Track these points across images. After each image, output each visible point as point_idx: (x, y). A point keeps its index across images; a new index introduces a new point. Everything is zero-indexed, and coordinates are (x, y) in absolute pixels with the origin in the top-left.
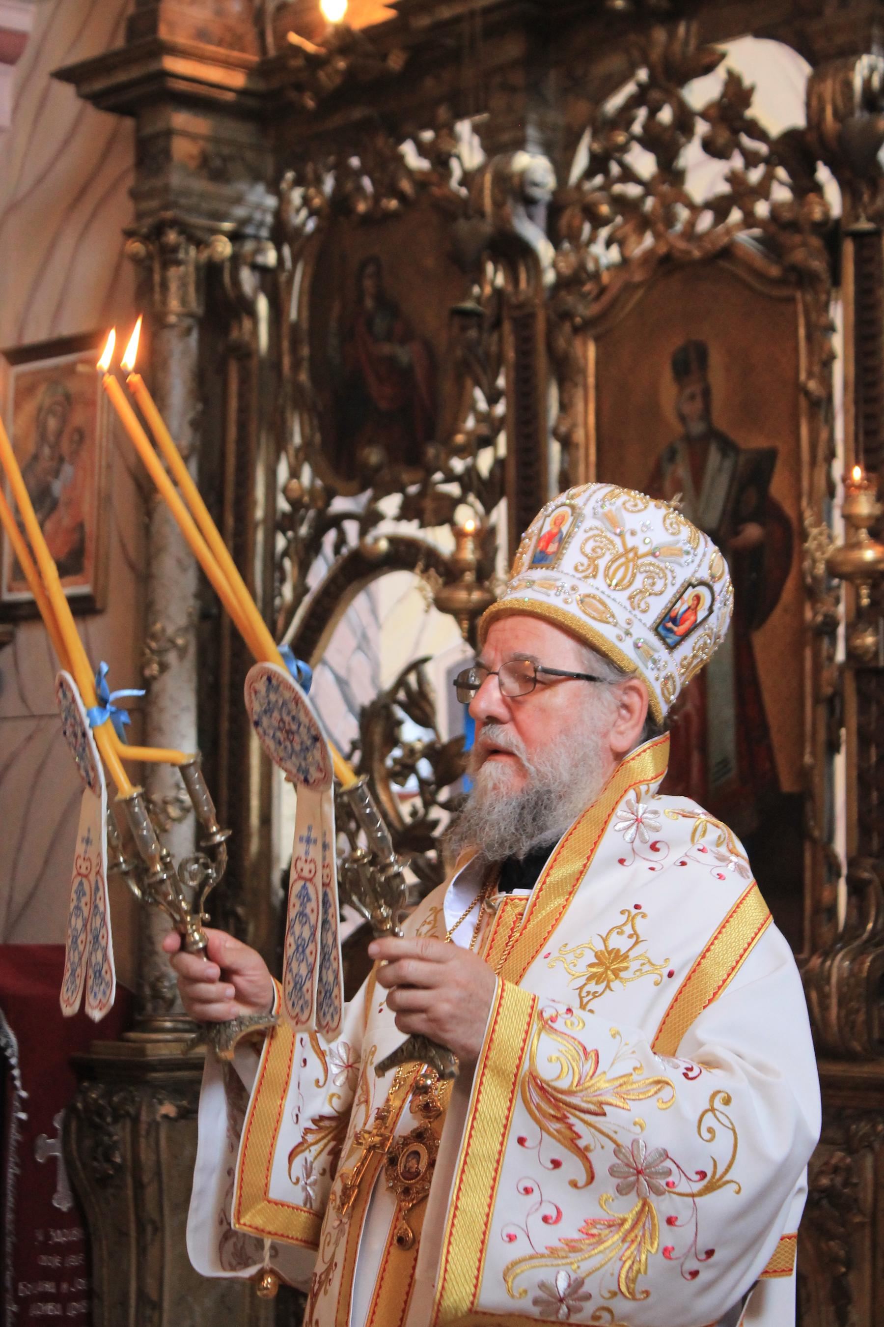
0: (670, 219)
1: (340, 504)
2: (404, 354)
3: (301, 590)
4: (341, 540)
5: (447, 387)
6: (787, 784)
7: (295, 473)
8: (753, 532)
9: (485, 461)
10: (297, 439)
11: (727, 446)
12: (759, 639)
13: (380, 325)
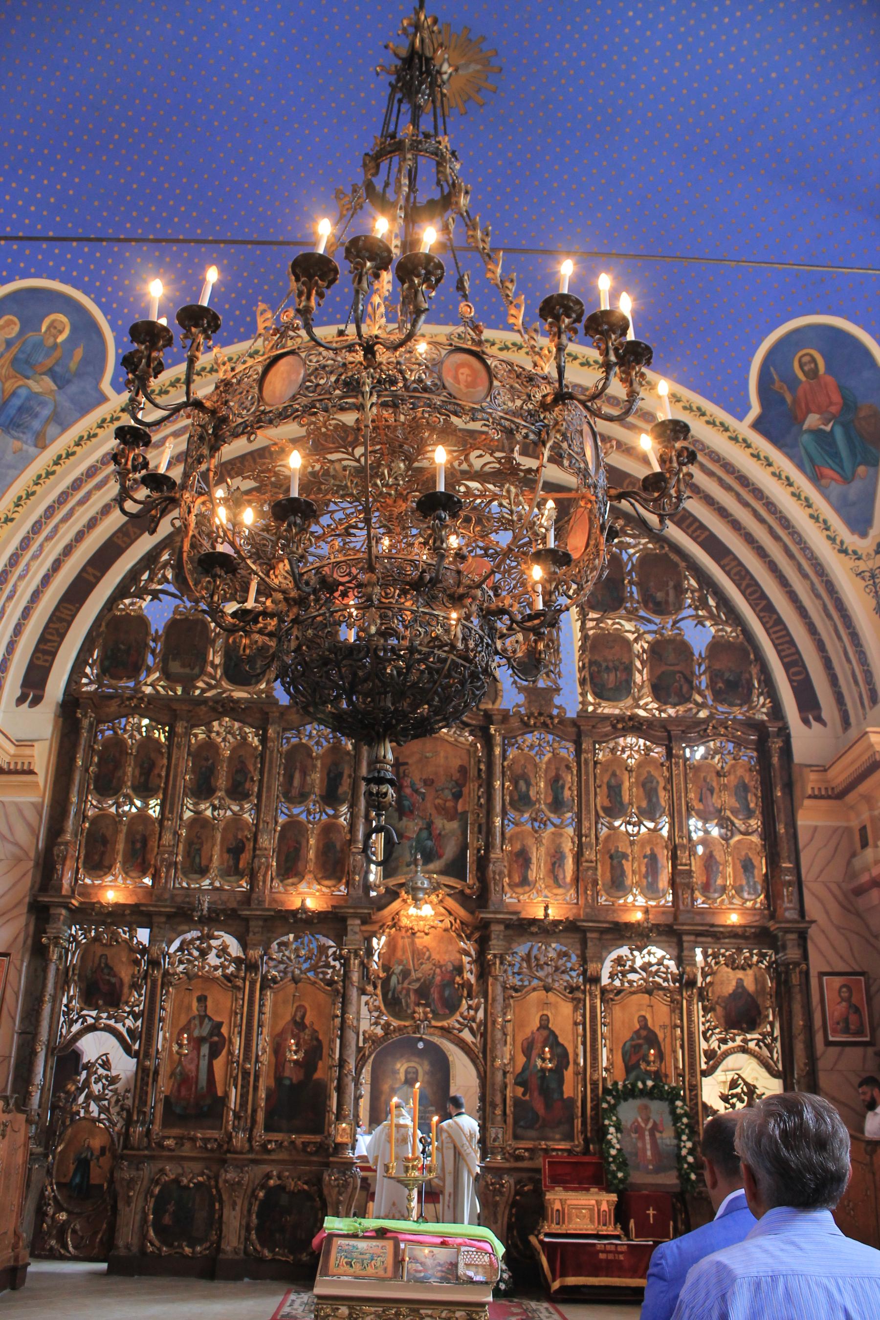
0: (203, 968)
1: (84, 1012)
2: (113, 980)
3: (69, 1031)
4: (85, 1020)
5: (126, 990)
6: (220, 1093)
7: (70, 1000)
8: (216, 1039)
9: (136, 1009)
10: (72, 993)
11: (210, 1019)
12: (215, 1062)
13: (106, 971)
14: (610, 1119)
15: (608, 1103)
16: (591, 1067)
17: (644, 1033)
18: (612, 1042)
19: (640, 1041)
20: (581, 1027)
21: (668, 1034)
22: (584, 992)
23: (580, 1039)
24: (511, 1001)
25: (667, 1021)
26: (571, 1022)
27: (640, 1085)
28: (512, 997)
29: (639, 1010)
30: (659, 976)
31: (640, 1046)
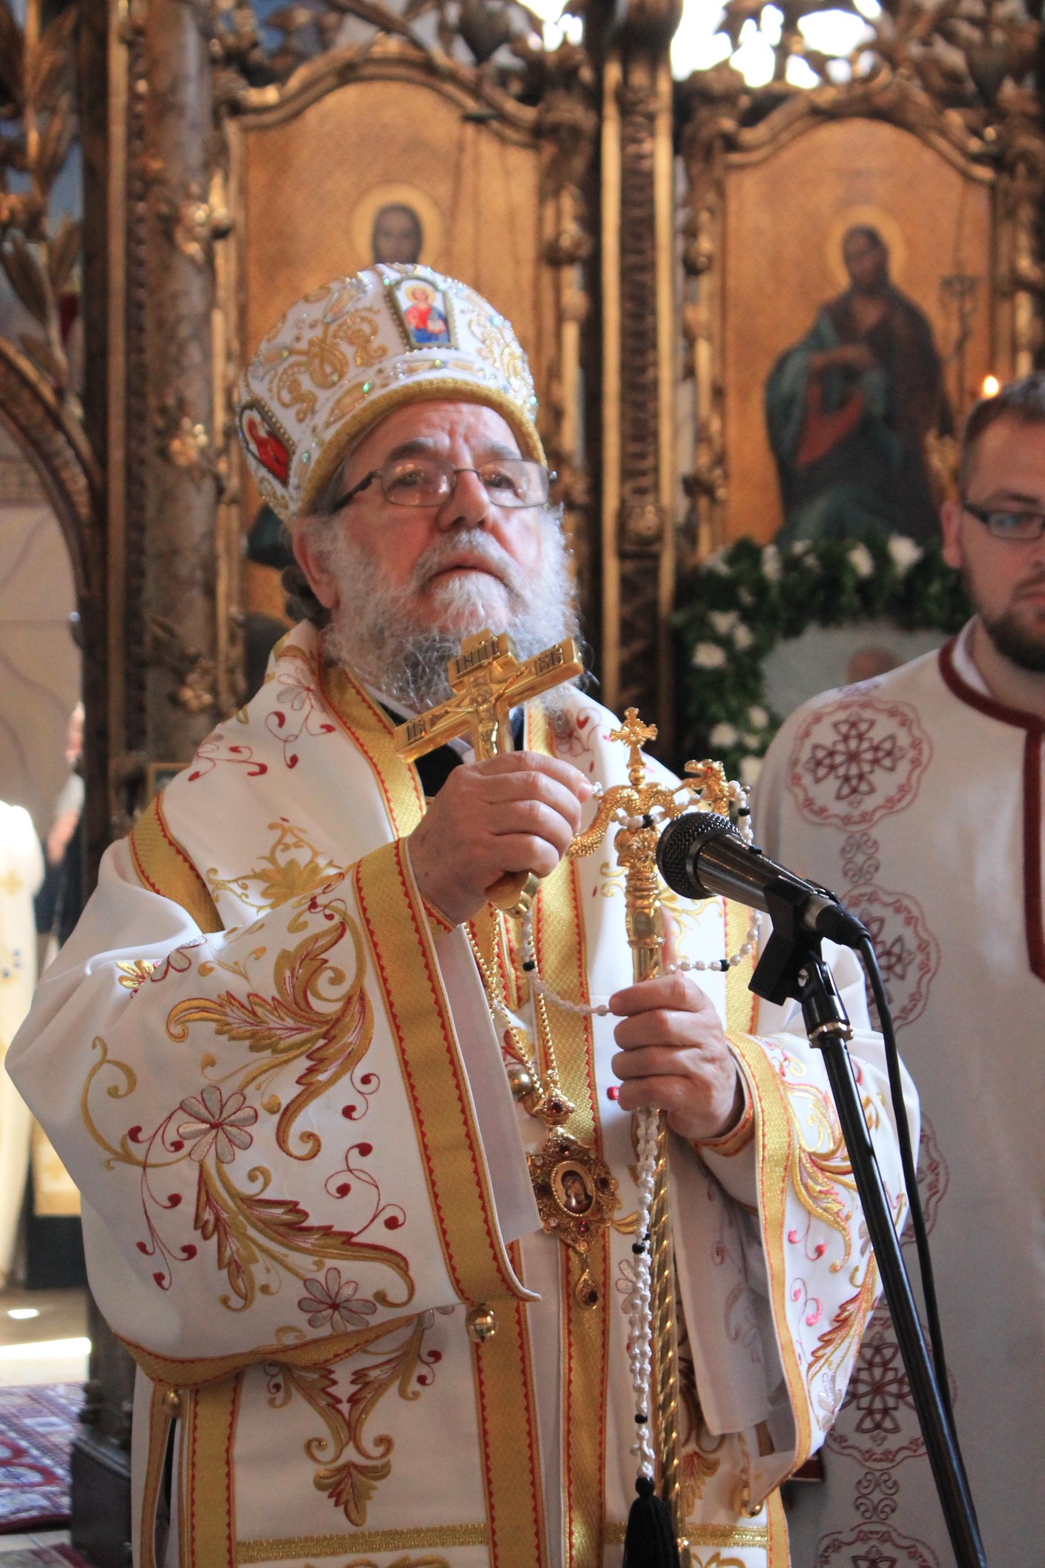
14: (737, 719)
15: (725, 642)
16: (627, 474)
17: (869, 314)
18: (721, 355)
19: (856, 353)
20: (572, 276)
21: (978, 322)
22: (594, 98)
23: (571, 334)
24: (232, 129)
25: (976, 261)
26: (528, 249)
27: (861, 561)
28: (237, 109)
29: (844, 204)
30: (951, 38)
31: (850, 374)
